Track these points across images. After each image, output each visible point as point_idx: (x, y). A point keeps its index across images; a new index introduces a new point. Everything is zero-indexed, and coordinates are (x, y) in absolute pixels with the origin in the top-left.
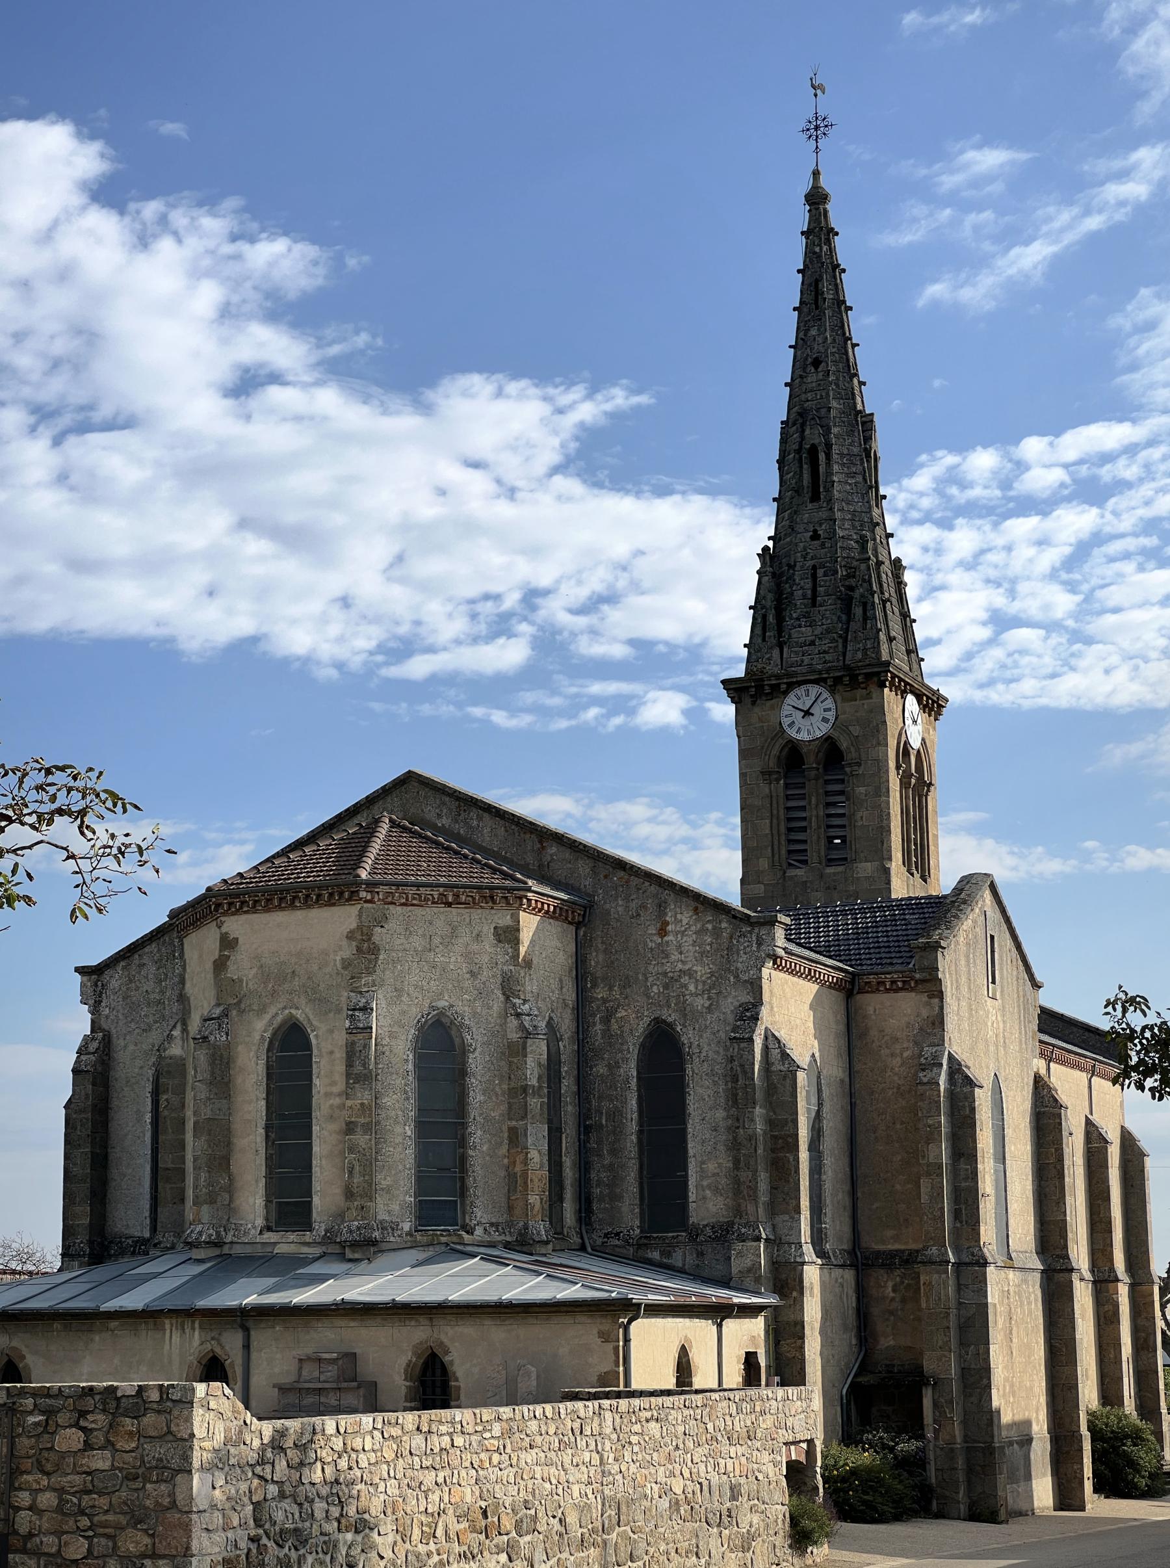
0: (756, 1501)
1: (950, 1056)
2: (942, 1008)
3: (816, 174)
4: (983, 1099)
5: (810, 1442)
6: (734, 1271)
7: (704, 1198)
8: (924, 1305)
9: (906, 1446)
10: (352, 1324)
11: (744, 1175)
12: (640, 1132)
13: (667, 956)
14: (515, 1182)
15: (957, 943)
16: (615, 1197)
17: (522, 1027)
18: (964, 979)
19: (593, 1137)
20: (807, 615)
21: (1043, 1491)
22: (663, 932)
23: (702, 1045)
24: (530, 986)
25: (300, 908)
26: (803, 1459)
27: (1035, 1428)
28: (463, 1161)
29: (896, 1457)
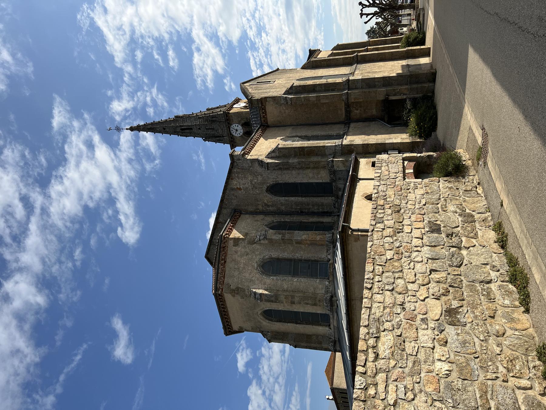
0: (439, 206)
1: (284, 94)
2: (270, 97)
3: (127, 129)
4: (297, 83)
5: (404, 159)
6: (344, 169)
7: (321, 177)
8: (361, 100)
9: (409, 105)
10: (356, 325)
11: (312, 165)
12: (302, 196)
13: (247, 188)
14: (313, 243)
15: (254, 93)
16: (322, 205)
17: (263, 239)
18: (265, 91)
19: (304, 211)
20: (216, 131)
21: (424, 61)
22: (240, 189)
23: (273, 178)
24: (253, 233)
25: (227, 310)
26: (412, 164)
27: (404, 64)
28: (307, 261)
29: (412, 108)
